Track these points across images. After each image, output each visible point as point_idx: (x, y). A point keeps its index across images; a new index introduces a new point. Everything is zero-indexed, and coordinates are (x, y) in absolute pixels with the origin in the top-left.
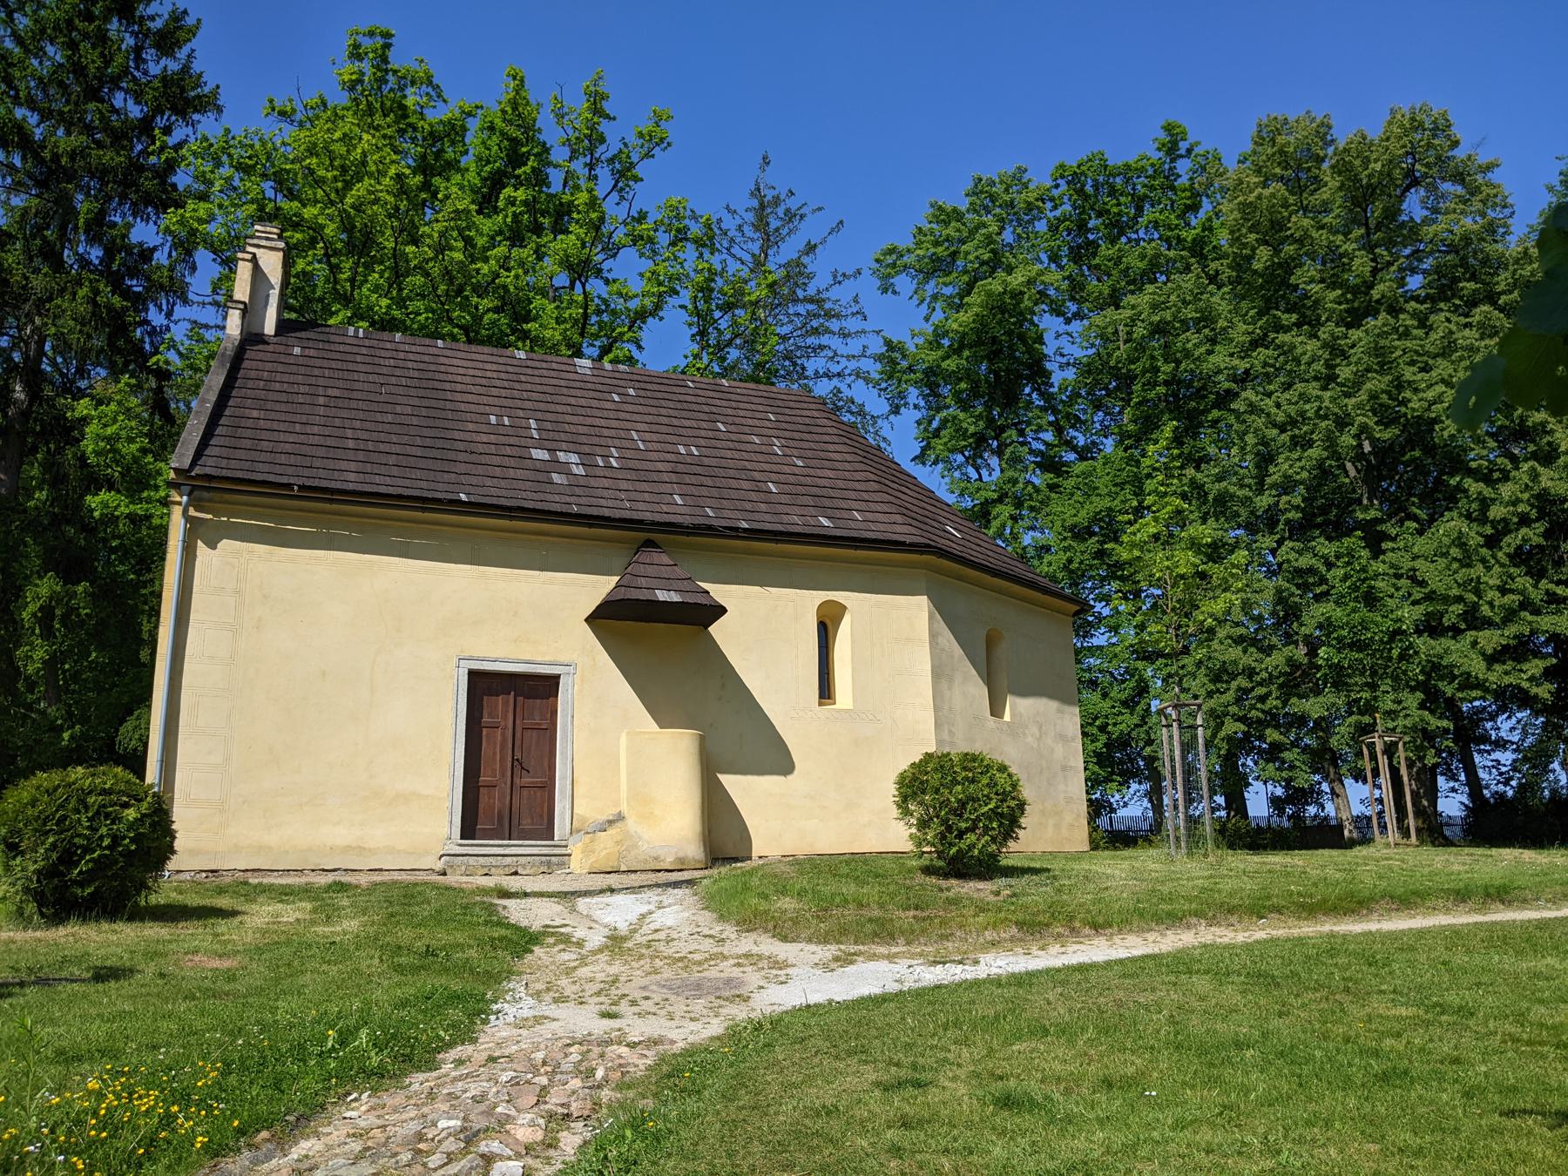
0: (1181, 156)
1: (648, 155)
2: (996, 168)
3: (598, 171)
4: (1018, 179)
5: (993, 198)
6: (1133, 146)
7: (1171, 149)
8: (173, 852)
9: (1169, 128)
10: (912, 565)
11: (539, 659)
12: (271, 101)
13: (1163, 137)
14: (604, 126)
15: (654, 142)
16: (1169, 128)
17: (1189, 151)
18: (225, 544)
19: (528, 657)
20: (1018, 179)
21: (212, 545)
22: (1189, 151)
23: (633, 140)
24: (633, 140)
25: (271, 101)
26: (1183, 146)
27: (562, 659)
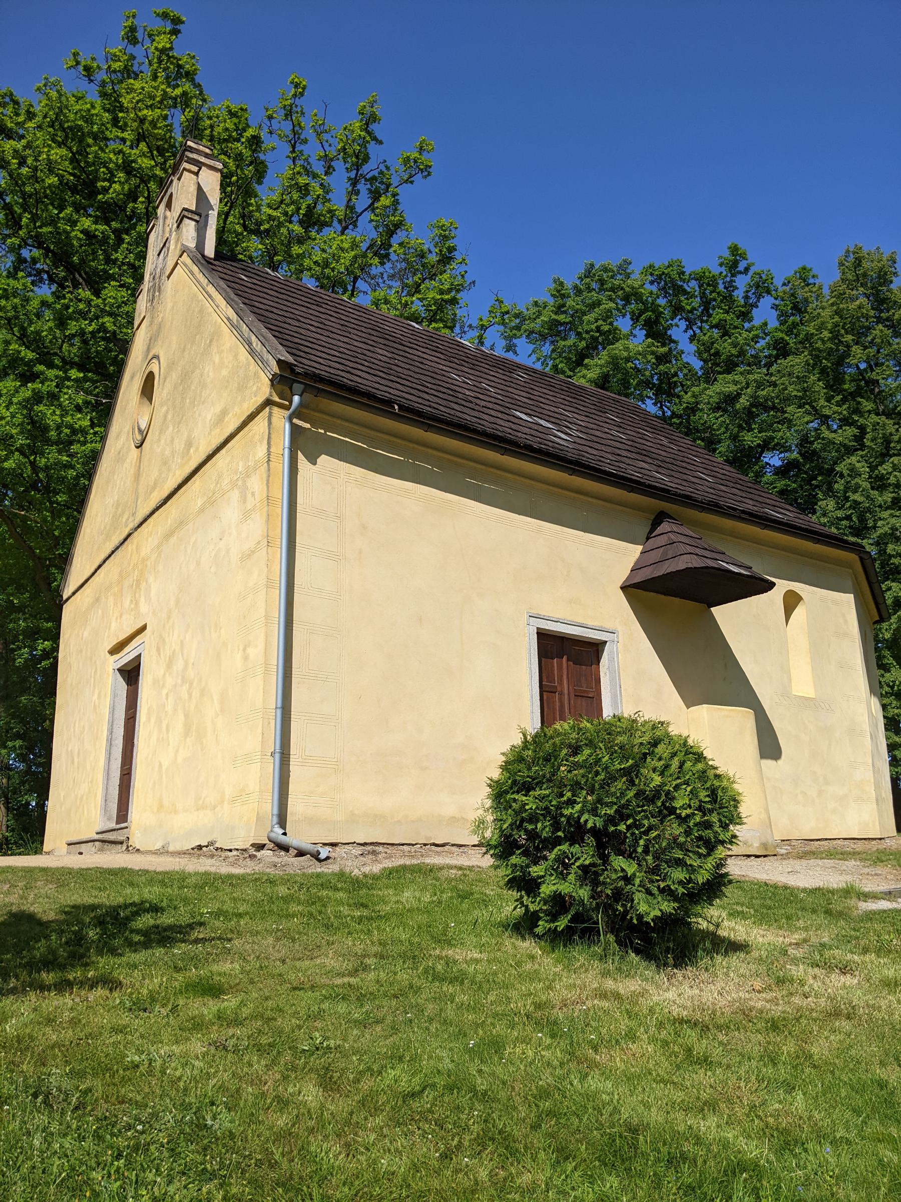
0: (740, 273)
1: (409, 181)
2: (607, 258)
3: (359, 187)
4: (624, 268)
5: (602, 282)
6: (702, 258)
7: (733, 267)
8: (501, 767)
9: (734, 250)
10: (838, 562)
11: (590, 623)
12: (75, 55)
13: (727, 254)
14: (372, 147)
15: (418, 169)
16: (734, 250)
17: (747, 270)
18: (323, 459)
19: (580, 620)
20: (624, 268)
21: (313, 461)
22: (747, 270)
23: (397, 165)
24: (397, 165)
25: (75, 55)
26: (742, 266)
27: (608, 626)
